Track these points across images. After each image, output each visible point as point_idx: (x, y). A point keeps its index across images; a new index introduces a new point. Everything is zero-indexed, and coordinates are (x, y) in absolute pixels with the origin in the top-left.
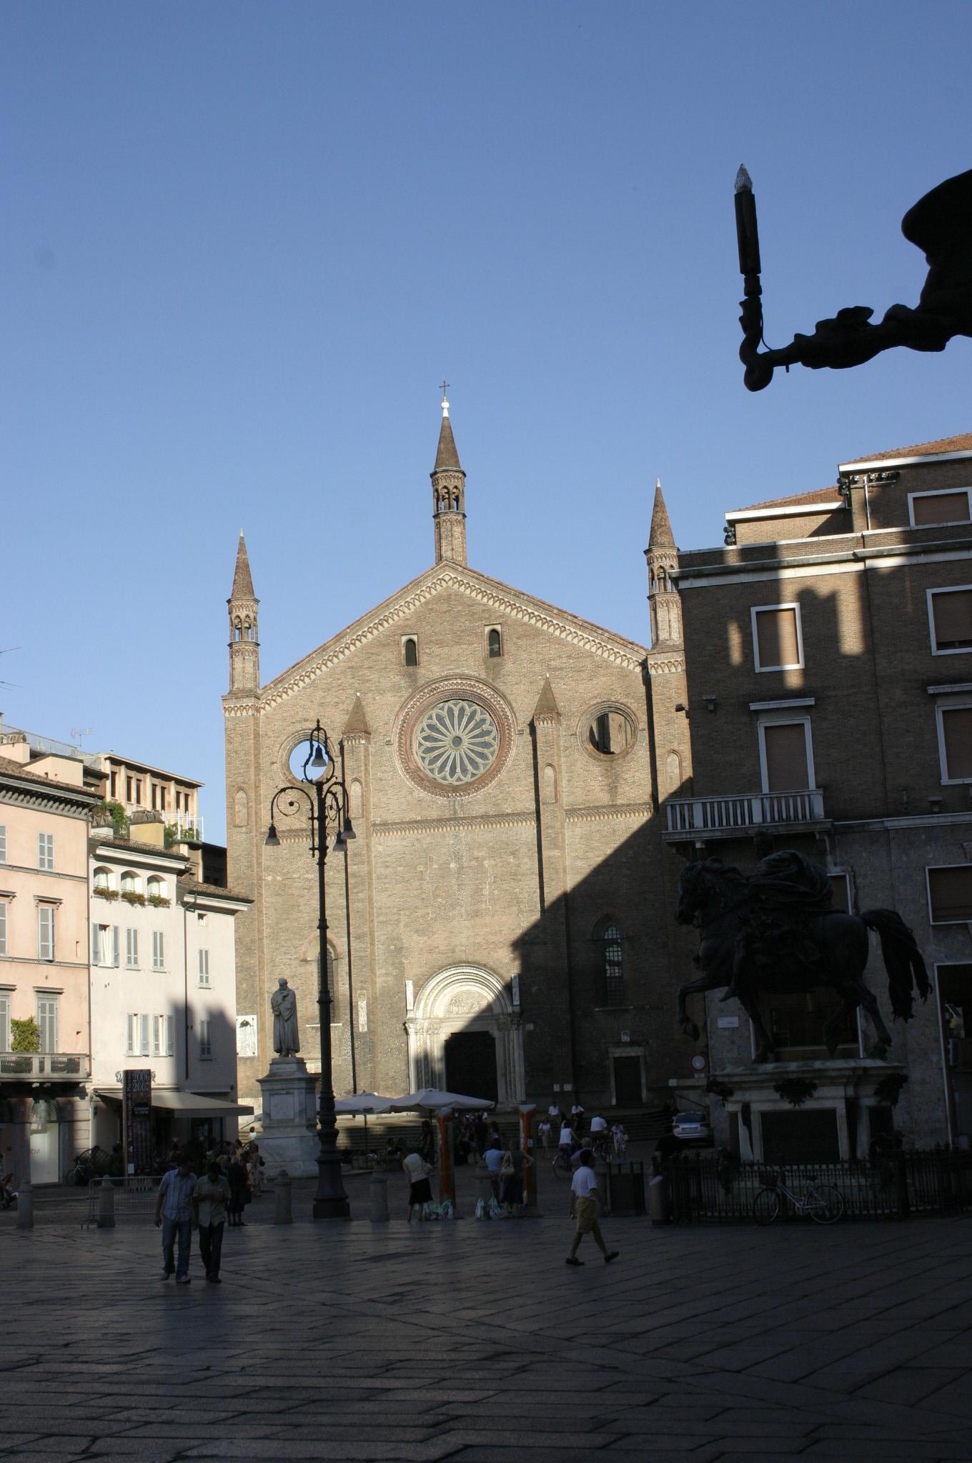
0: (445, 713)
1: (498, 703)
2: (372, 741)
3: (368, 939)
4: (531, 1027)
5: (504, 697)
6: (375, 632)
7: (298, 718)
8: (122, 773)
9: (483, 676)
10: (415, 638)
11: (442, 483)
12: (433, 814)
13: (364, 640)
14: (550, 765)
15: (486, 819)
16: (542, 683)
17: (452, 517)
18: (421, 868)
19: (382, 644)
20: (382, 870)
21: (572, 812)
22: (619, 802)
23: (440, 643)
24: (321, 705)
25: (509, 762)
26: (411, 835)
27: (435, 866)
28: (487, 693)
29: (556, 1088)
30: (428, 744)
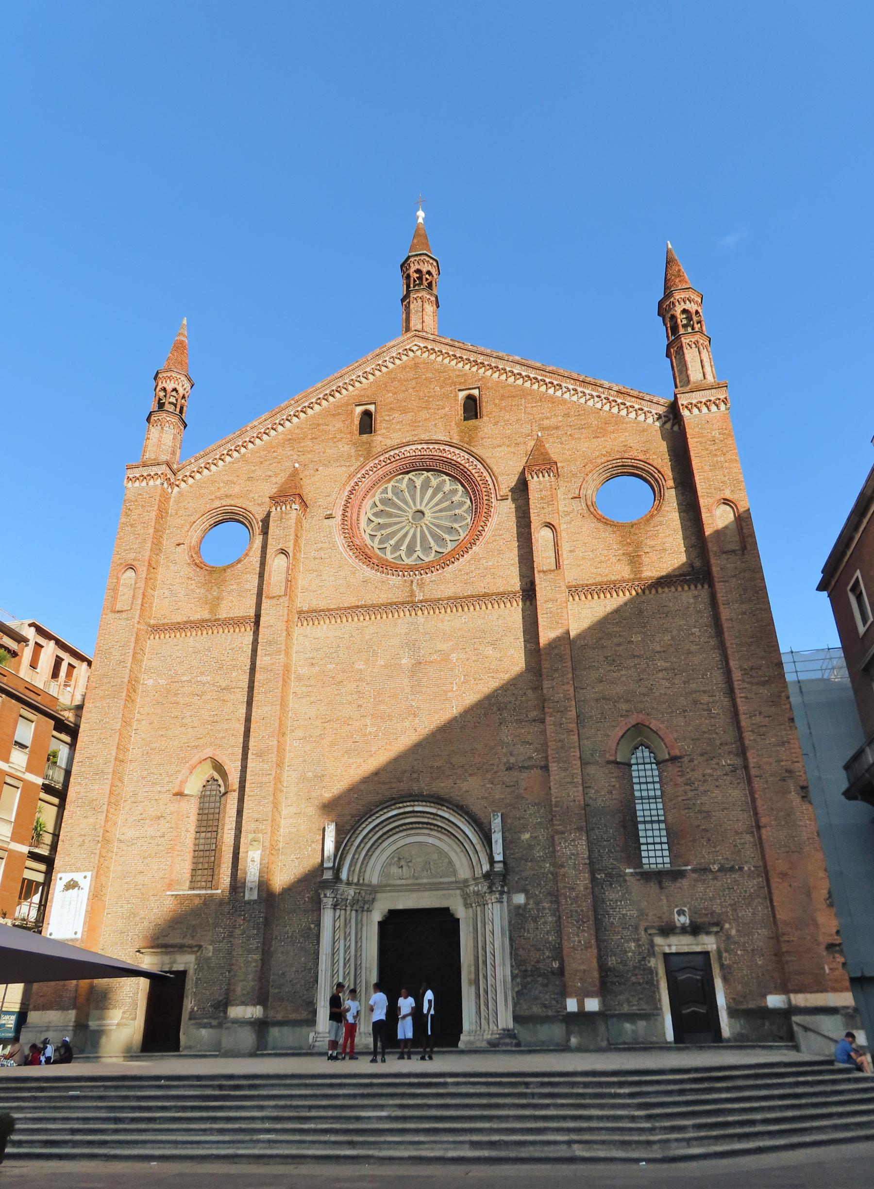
0: (404, 486)
1: (475, 469)
2: (308, 515)
3: (273, 757)
4: (520, 899)
5: (481, 460)
6: (324, 403)
7: (218, 494)
8: (50, 649)
9: (456, 440)
10: (372, 408)
11: (413, 268)
12: (383, 597)
13: (309, 411)
14: (549, 525)
15: (460, 602)
16: (532, 443)
17: (425, 294)
19: (333, 414)
20: (304, 671)
21: (574, 590)
23: (404, 411)
24: (250, 479)
25: (488, 533)
26: (350, 626)
28: (460, 457)
29: (572, 1005)
30: (381, 521)
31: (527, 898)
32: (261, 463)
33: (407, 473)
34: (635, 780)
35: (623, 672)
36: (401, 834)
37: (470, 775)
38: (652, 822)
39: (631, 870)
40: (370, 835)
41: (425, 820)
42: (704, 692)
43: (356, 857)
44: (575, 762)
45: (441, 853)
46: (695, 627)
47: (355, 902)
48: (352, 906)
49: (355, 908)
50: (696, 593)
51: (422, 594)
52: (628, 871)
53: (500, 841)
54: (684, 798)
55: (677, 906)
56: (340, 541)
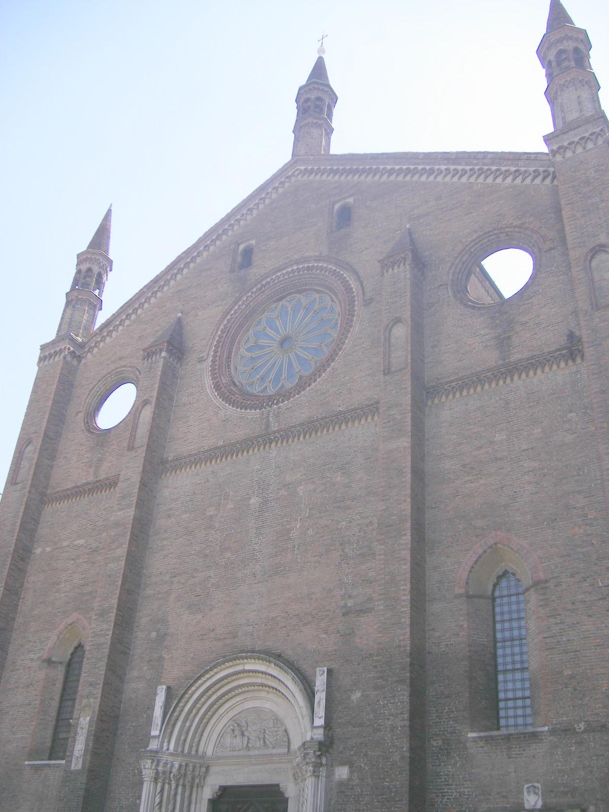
4: (342, 772)
15: (311, 427)
18: (211, 511)
22: (515, 357)
27: (231, 506)
31: (351, 772)
32: (152, 320)
33: (281, 299)
34: (498, 618)
35: (482, 482)
36: (238, 699)
37: (305, 624)
38: (514, 670)
39: (474, 735)
40: (203, 700)
41: (259, 681)
42: (579, 492)
43: (188, 724)
44: (403, 598)
45: (277, 720)
46: (571, 411)
47: (182, 775)
48: (178, 781)
49: (181, 782)
50: (574, 369)
51: (277, 424)
52: (470, 735)
53: (323, 702)
54: (546, 635)
55: (527, 781)
56: (208, 382)
